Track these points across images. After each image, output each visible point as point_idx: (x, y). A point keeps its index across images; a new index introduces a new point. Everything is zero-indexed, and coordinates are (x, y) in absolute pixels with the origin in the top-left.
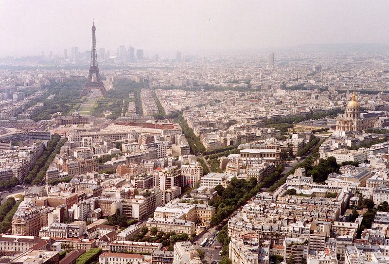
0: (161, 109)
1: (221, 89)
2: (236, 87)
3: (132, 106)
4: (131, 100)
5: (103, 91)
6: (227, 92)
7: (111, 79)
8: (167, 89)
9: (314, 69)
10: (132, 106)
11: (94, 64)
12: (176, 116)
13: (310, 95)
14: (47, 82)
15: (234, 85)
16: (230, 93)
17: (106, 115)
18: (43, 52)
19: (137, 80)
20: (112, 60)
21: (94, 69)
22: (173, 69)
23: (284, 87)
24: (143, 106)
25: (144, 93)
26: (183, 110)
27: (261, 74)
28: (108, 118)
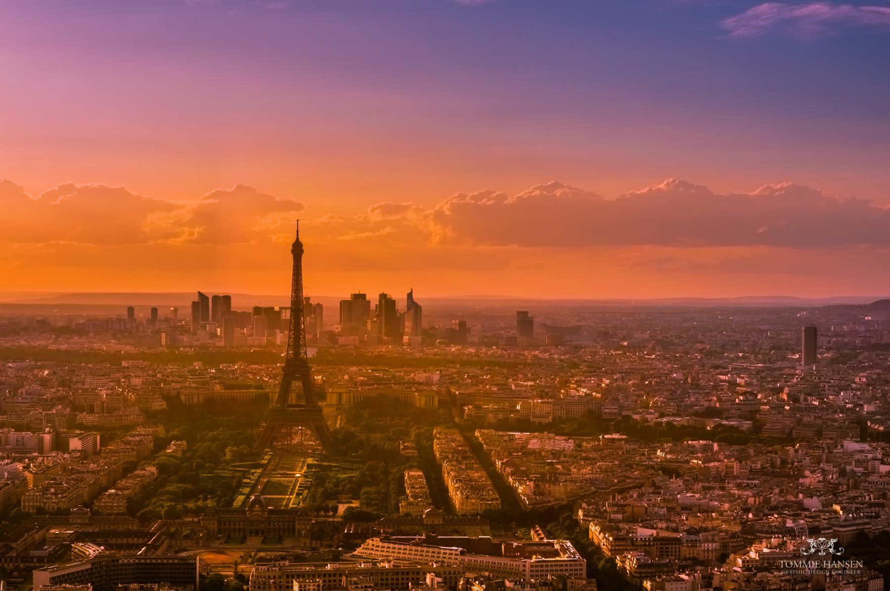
0: (507, 493)
2: (716, 427)
3: (413, 477)
5: (321, 432)
7: (340, 395)
8: (505, 425)
10: (413, 477)
11: (297, 353)
14: (159, 405)
17: (342, 508)
18: (131, 310)
19: (420, 401)
20: (332, 337)
21: (296, 367)
24: (451, 485)
27: (786, 390)
28: (352, 516)
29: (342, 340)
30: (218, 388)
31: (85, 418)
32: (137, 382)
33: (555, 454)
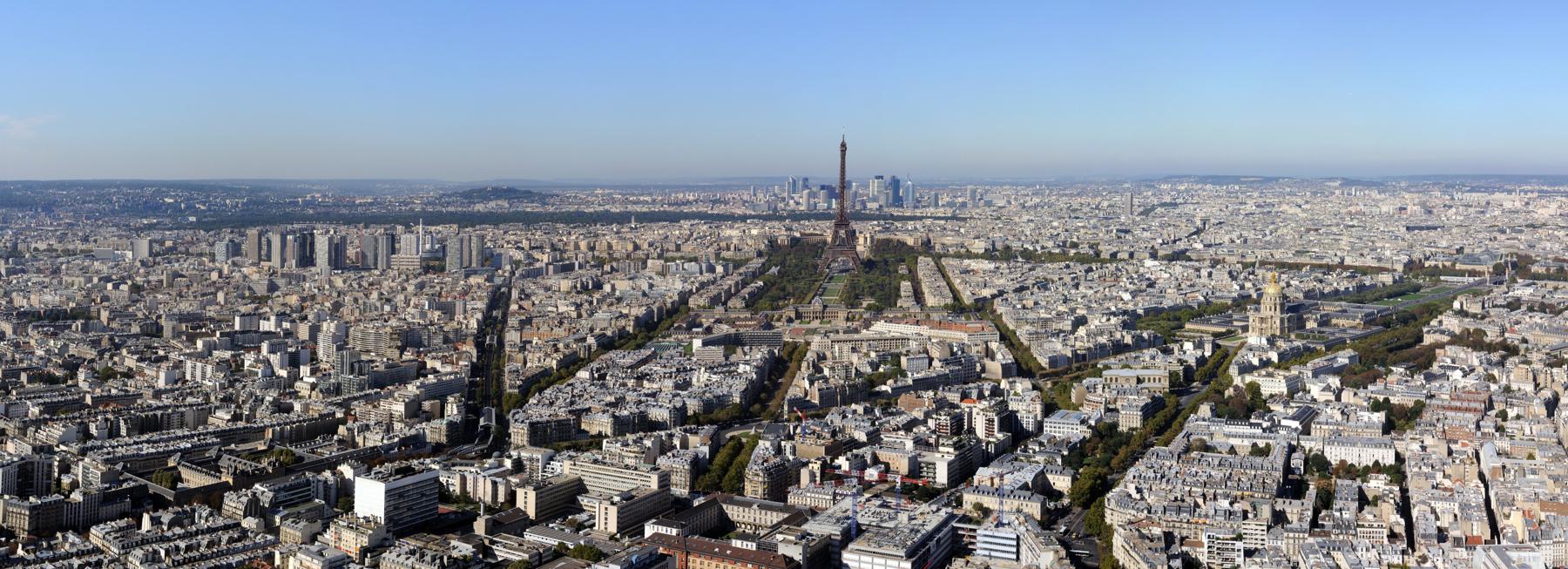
1: (1051, 258)
3: (906, 286)
4: (903, 277)
6: (1063, 264)
8: (958, 256)
9: (1199, 223)
10: (906, 286)
12: (982, 308)
13: (1198, 270)
15: (1073, 252)
16: (1068, 267)
17: (865, 304)
19: (910, 242)
22: (964, 219)
23: (1154, 256)
24: (926, 290)
25: (924, 265)
26: (994, 297)
28: (869, 308)
29: (869, 205)
30: (798, 235)
31: (725, 254)
32: (754, 232)
33: (985, 272)
